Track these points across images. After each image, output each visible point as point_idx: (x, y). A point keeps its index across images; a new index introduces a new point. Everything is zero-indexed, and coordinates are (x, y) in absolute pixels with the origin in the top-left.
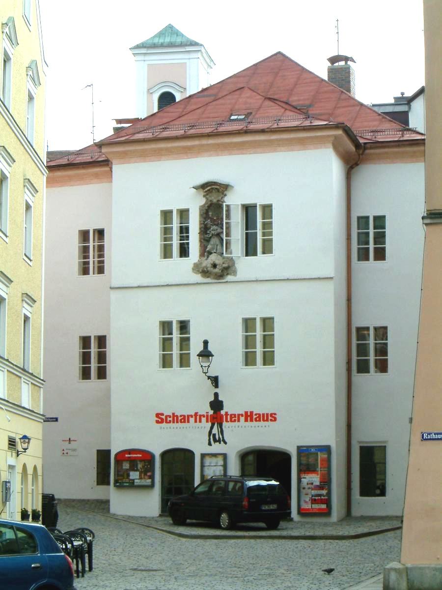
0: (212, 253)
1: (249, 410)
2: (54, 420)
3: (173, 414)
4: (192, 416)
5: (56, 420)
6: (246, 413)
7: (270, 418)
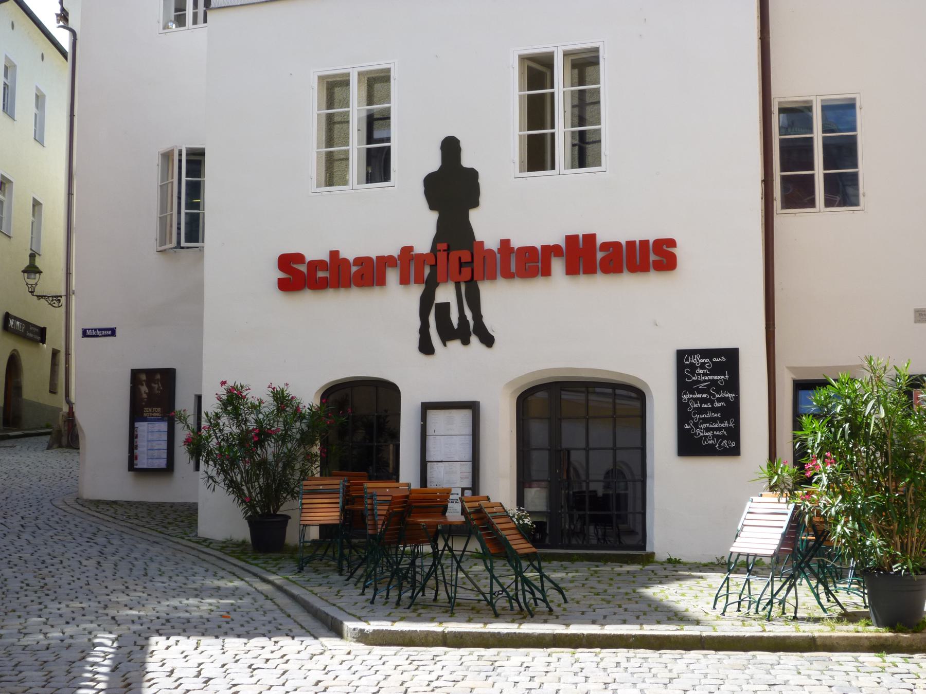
1: (580, 230)
2: (109, 333)
3: (334, 254)
5: (112, 332)
7: (653, 257)
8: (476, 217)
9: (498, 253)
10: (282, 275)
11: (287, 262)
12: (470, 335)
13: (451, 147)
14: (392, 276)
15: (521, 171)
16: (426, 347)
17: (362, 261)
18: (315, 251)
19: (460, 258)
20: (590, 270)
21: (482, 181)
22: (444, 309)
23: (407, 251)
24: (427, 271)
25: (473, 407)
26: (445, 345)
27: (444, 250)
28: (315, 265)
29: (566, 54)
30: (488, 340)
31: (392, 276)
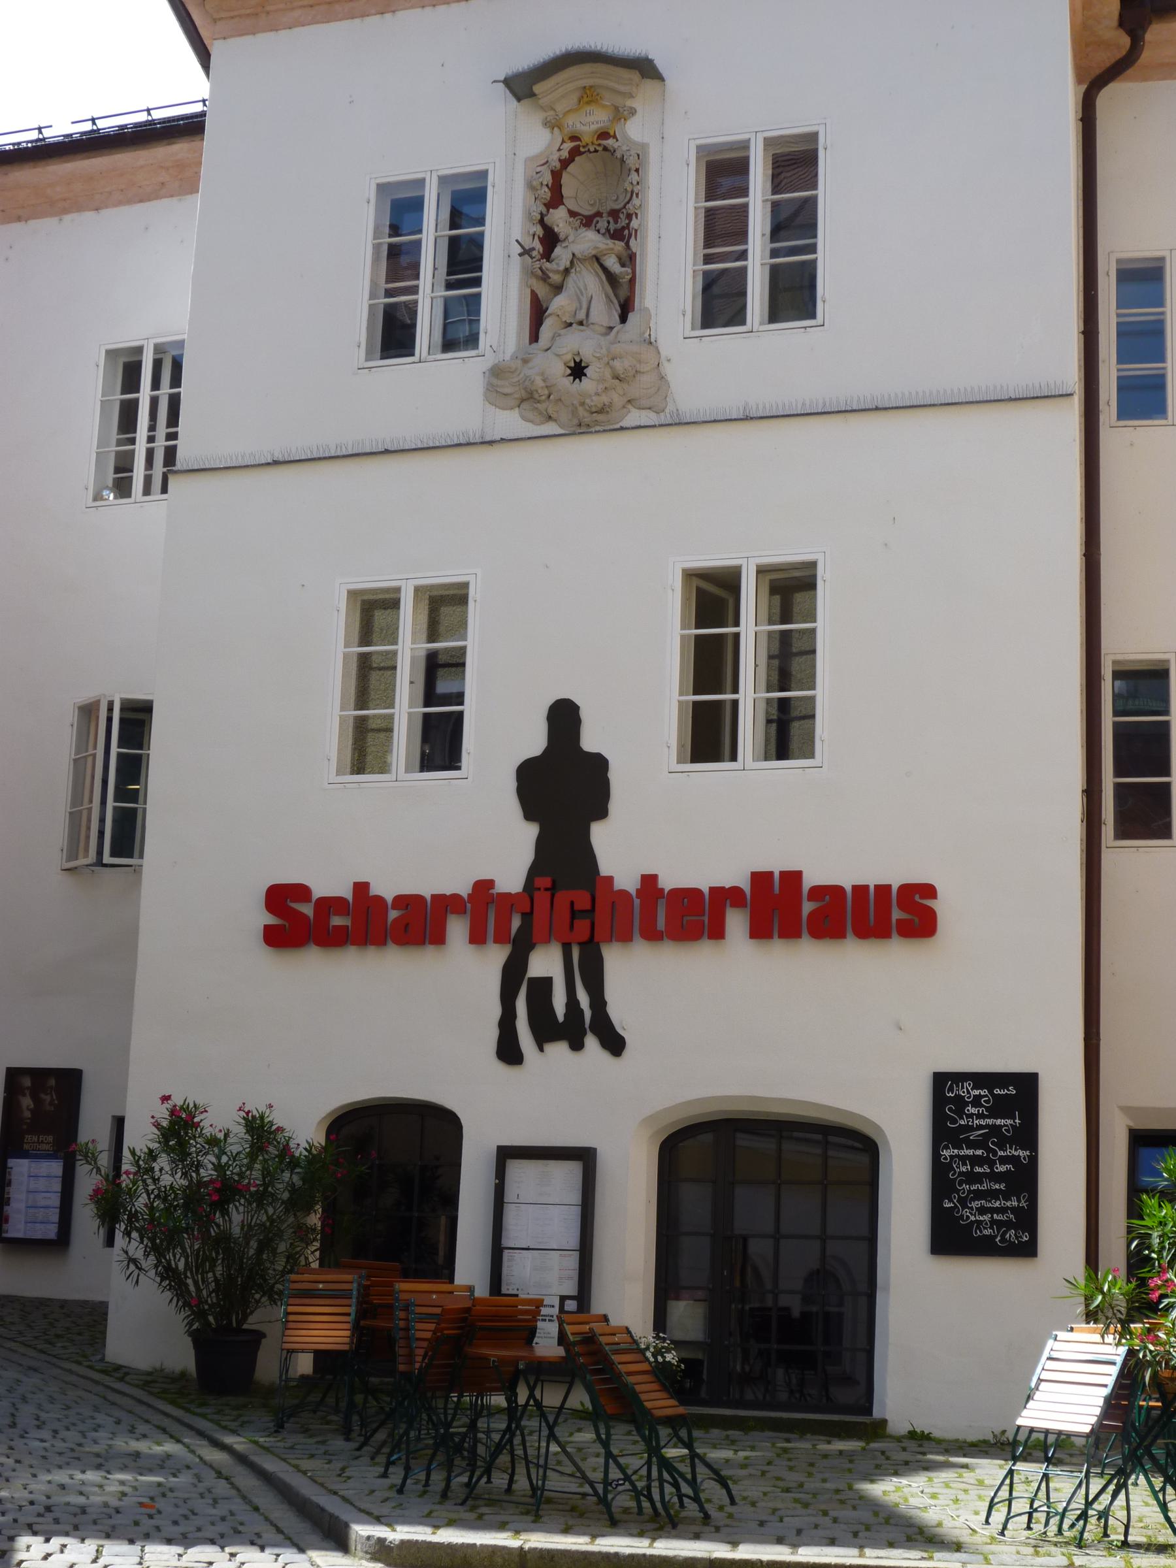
1: (776, 864)
3: (361, 888)
6: (760, 879)
7: (896, 914)
8: (601, 835)
9: (637, 897)
10: (271, 920)
12: (585, 1034)
15: (679, 762)
16: (509, 1052)
17: (405, 902)
19: (572, 904)
20: (791, 932)
21: (615, 776)
22: (542, 987)
23: (483, 887)
24: (516, 923)
25: (585, 1157)
26: (541, 1049)
27: (546, 889)
28: (328, 905)
29: (761, 571)
30: (614, 1044)
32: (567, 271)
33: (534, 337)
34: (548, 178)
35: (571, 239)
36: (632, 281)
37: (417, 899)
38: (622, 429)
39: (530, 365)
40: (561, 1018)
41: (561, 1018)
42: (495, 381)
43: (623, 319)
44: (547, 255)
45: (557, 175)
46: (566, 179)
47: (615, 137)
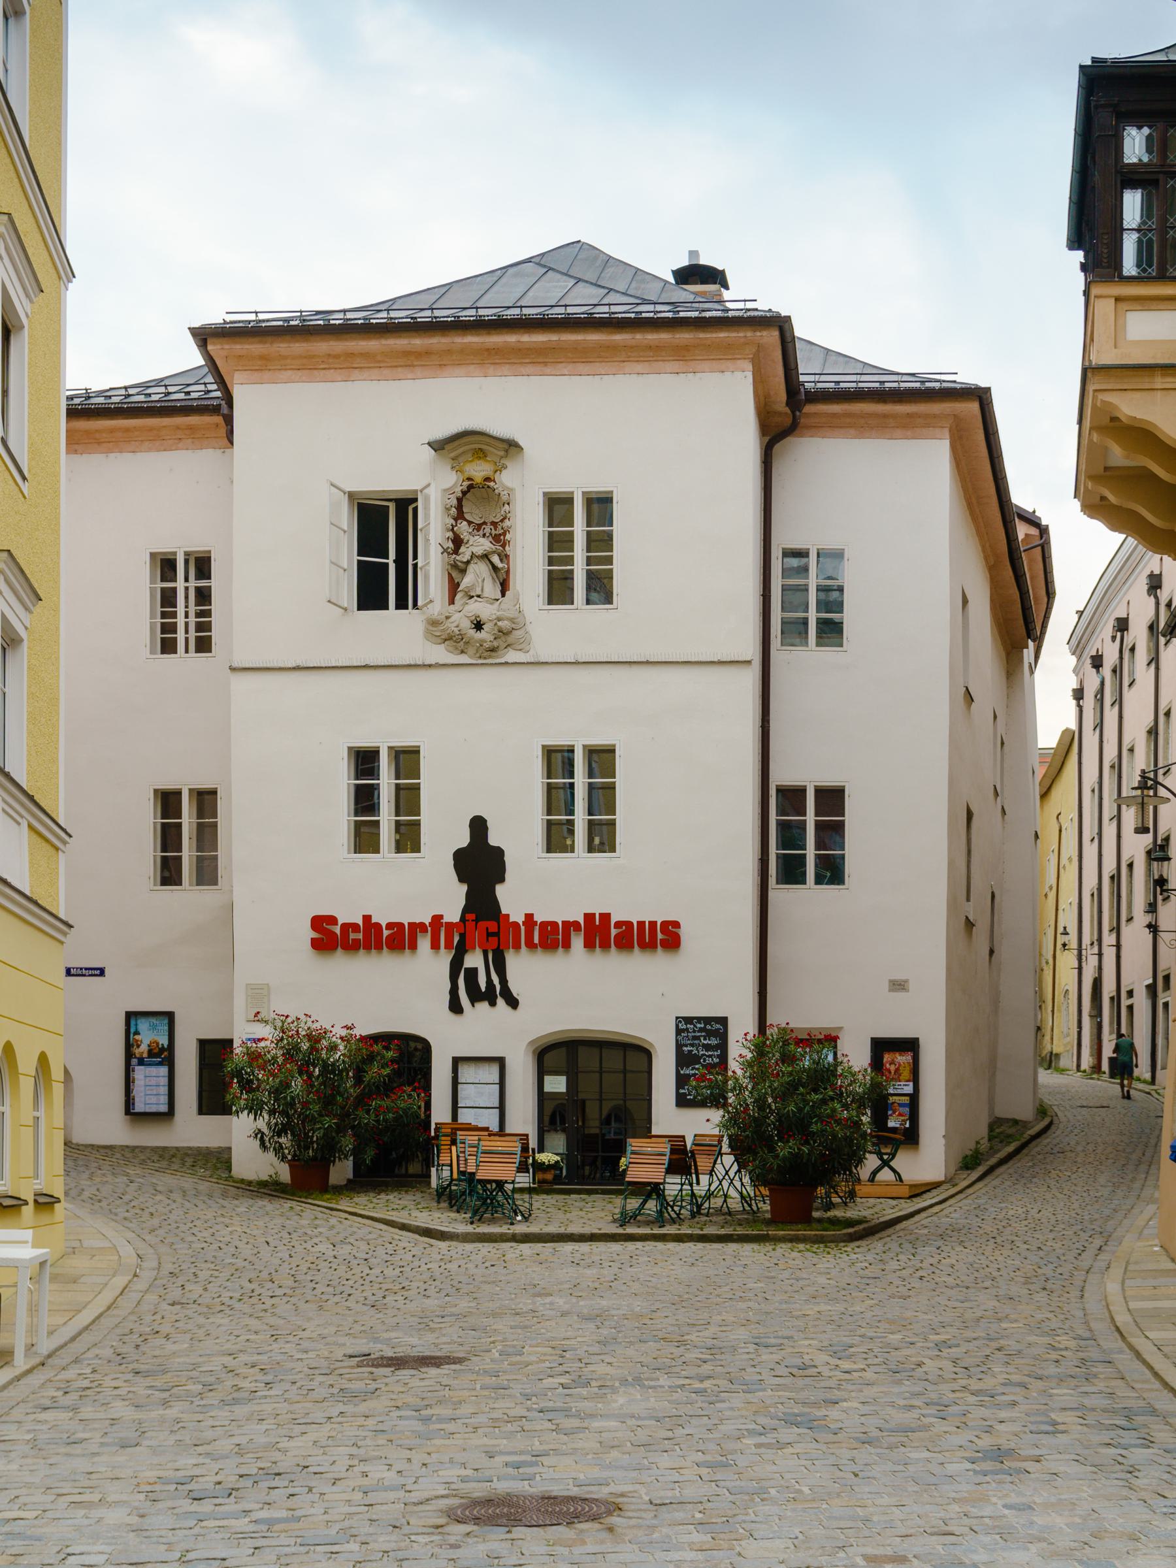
0: (473, 597)
1: (597, 910)
3: (367, 918)
4: (422, 927)
6: (589, 917)
7: (660, 936)
8: (502, 892)
10: (315, 935)
11: (320, 923)
12: (496, 997)
13: (478, 826)
14: (424, 943)
16: (455, 1007)
18: (349, 914)
20: (605, 945)
21: (507, 859)
22: (472, 974)
23: (437, 919)
24: (456, 939)
25: (501, 1062)
26: (473, 1006)
30: (513, 1003)
31: (424, 943)
32: (468, 562)
33: (452, 601)
34: (455, 502)
35: (471, 543)
36: (508, 572)
37: (400, 926)
38: (506, 663)
39: (450, 620)
40: (483, 990)
41: (483, 989)
42: (431, 628)
43: (503, 595)
44: (456, 551)
45: (459, 500)
46: (464, 503)
47: (494, 481)
